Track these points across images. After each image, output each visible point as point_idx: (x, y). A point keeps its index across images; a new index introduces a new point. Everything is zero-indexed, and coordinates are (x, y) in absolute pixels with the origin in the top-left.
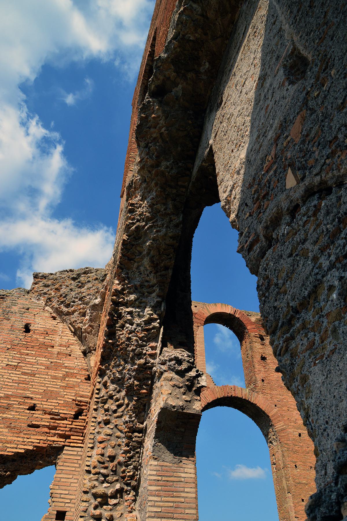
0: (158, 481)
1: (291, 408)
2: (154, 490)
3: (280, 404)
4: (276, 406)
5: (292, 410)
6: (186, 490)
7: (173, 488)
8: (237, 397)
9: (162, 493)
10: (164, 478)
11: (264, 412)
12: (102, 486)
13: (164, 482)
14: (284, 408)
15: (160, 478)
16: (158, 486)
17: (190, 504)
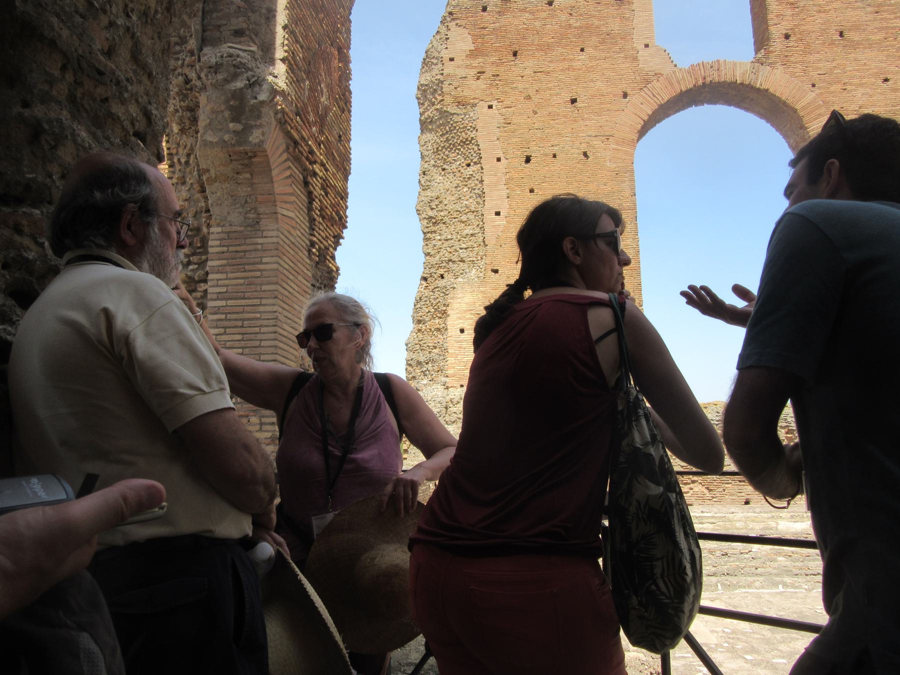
0: (223, 253)
1: (851, 84)
2: (217, 266)
3: (824, 81)
4: (814, 86)
5: (854, 87)
6: (264, 260)
7: (244, 260)
8: (725, 82)
9: (228, 269)
10: (231, 249)
11: (784, 103)
12: (188, 268)
13: (231, 254)
14: (832, 89)
15: (225, 249)
16: (223, 259)
17: (270, 279)
